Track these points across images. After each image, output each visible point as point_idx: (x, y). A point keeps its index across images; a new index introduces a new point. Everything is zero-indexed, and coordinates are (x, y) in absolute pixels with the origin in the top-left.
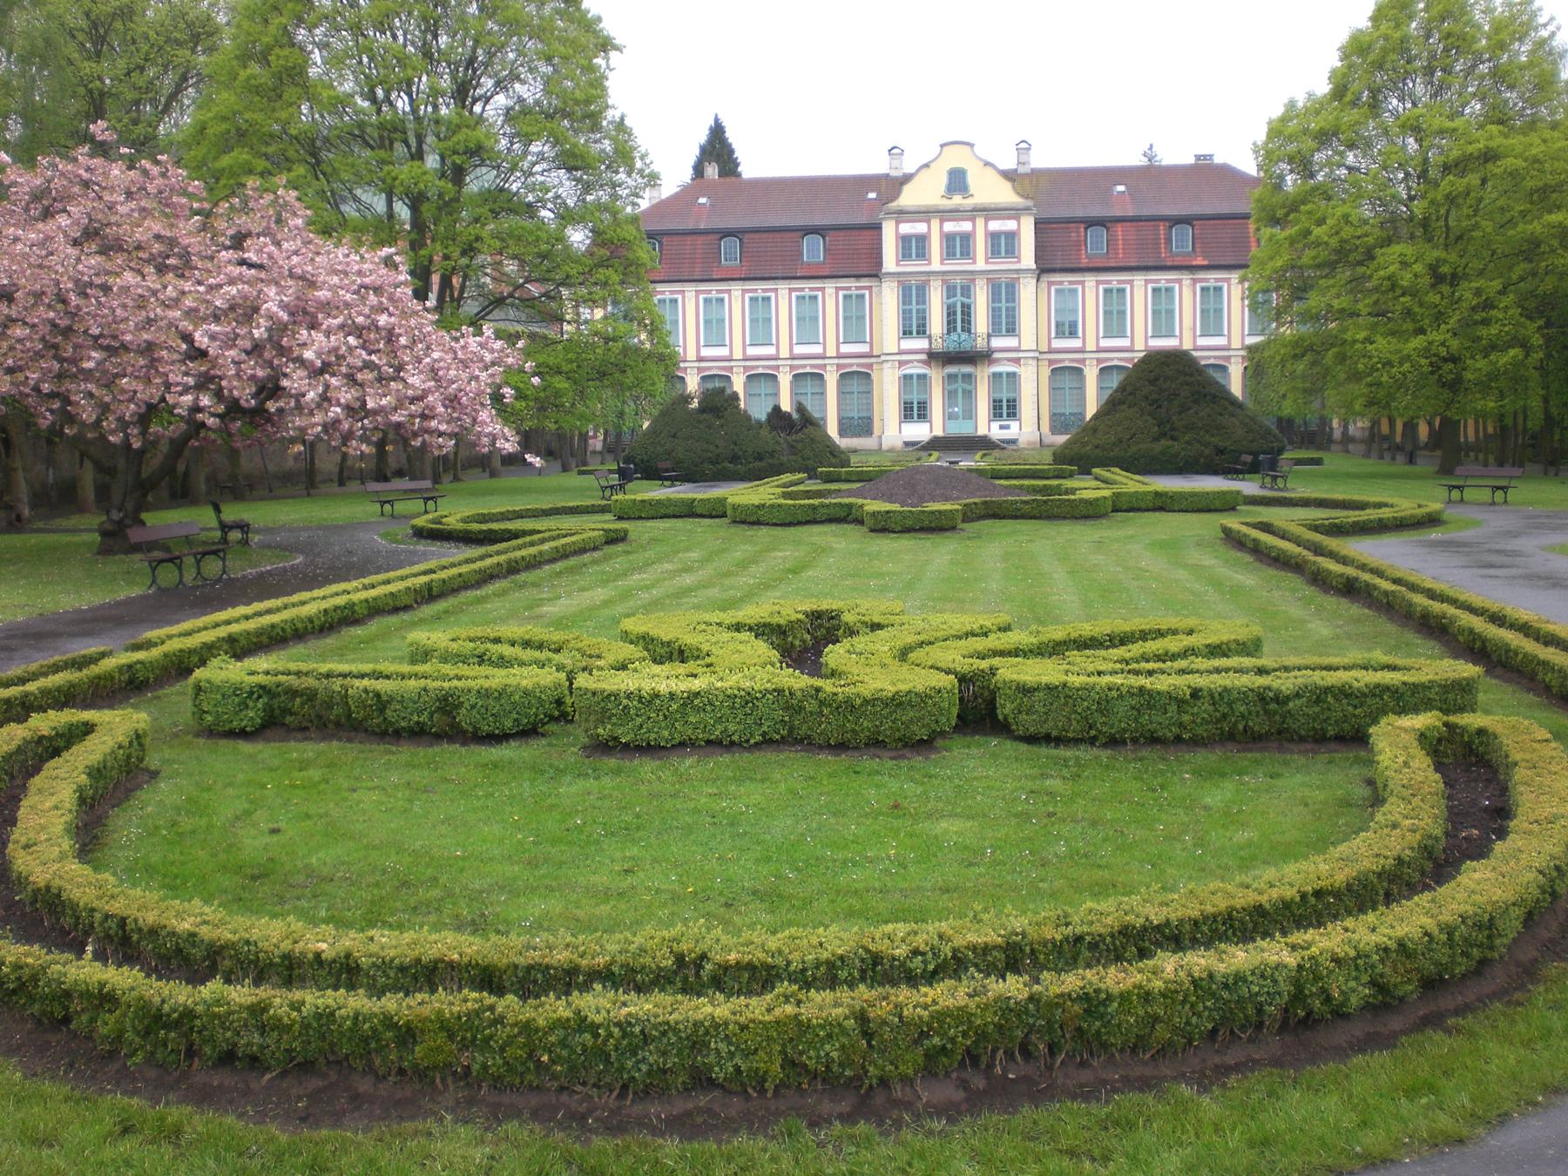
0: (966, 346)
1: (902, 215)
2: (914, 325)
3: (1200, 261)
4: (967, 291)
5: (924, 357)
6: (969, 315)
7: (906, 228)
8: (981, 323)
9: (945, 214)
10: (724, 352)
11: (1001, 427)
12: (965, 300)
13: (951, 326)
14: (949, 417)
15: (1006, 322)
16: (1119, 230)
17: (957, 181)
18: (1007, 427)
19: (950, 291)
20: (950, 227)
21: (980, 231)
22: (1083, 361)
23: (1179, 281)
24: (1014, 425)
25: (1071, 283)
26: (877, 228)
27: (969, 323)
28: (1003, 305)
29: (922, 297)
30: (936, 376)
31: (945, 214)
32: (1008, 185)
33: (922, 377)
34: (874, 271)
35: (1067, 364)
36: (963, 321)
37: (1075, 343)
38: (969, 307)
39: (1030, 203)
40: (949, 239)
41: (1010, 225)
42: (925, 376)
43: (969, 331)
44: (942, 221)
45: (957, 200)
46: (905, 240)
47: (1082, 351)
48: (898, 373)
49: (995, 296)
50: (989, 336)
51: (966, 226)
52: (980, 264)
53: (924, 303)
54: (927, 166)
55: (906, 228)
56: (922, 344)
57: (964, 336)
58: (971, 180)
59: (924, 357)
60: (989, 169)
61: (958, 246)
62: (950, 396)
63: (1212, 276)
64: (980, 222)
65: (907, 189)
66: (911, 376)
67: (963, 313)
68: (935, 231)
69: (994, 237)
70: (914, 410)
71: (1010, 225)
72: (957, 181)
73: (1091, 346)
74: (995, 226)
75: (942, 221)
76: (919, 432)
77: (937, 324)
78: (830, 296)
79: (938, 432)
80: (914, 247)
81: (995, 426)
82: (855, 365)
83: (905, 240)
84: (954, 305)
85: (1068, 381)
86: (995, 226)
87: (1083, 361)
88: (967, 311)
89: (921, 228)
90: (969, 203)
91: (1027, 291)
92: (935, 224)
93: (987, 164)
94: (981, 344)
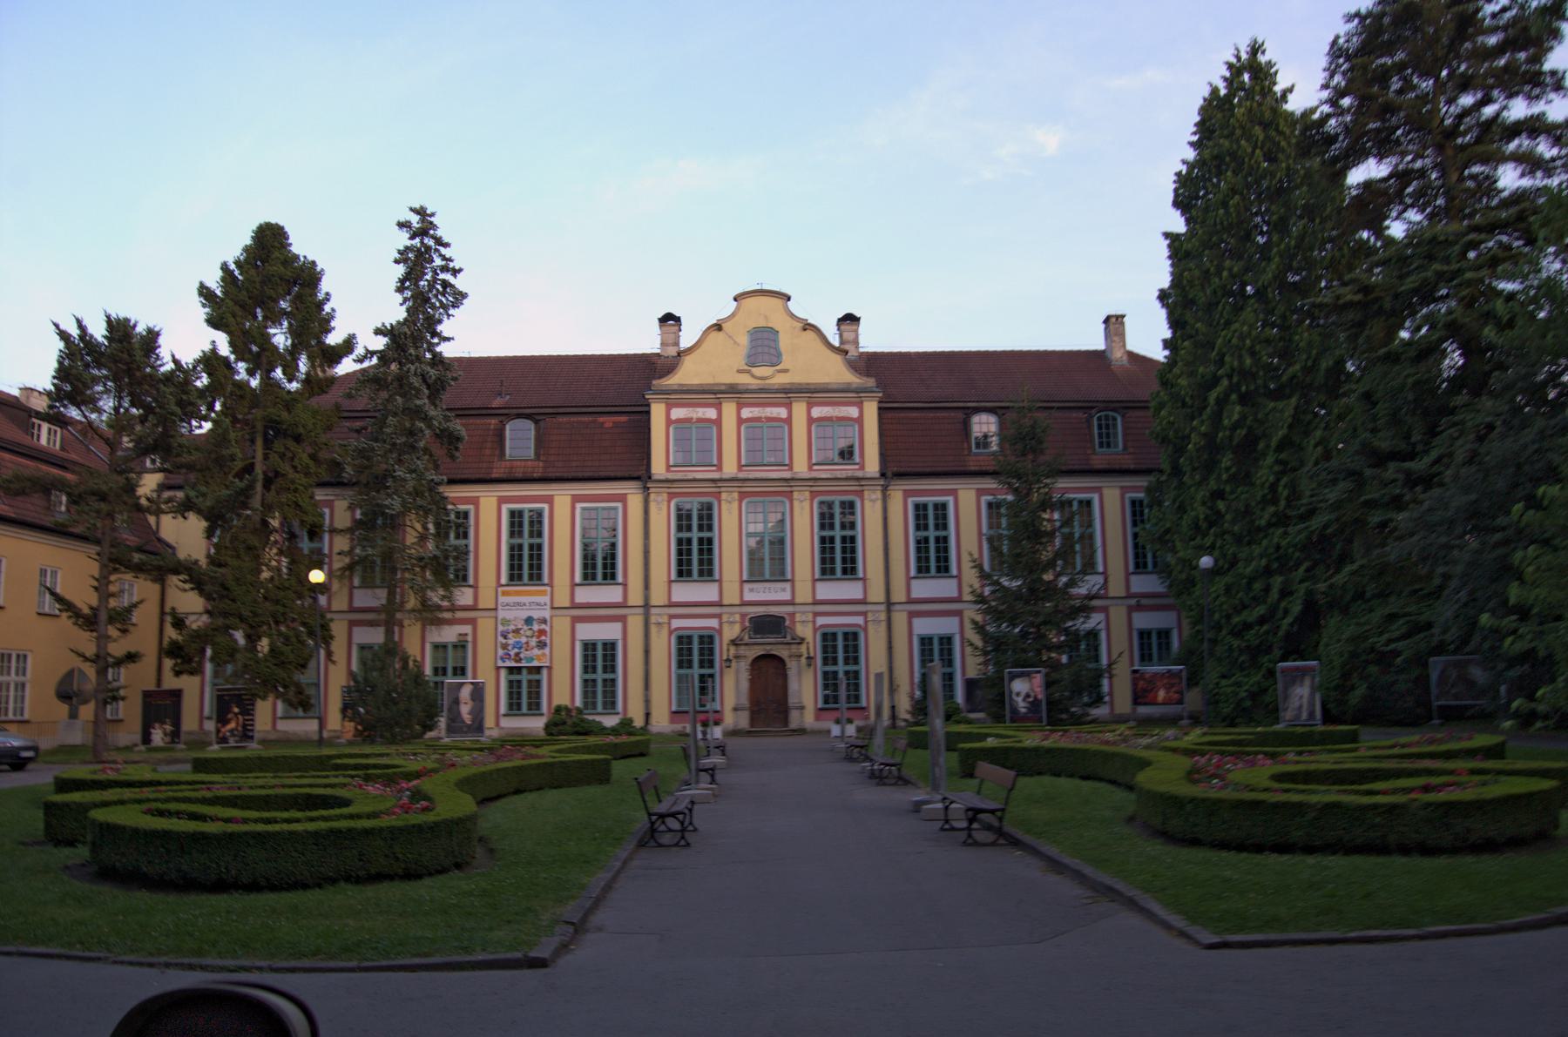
17: (764, 345)
26: (648, 413)
32: (838, 358)
34: (640, 474)
39: (871, 382)
44: (740, 406)
58: (784, 342)
60: (810, 334)
64: (799, 409)
72: (764, 345)
75: (740, 406)
78: (565, 512)
90: (780, 380)
91: (870, 512)
92: (729, 409)
93: (808, 327)
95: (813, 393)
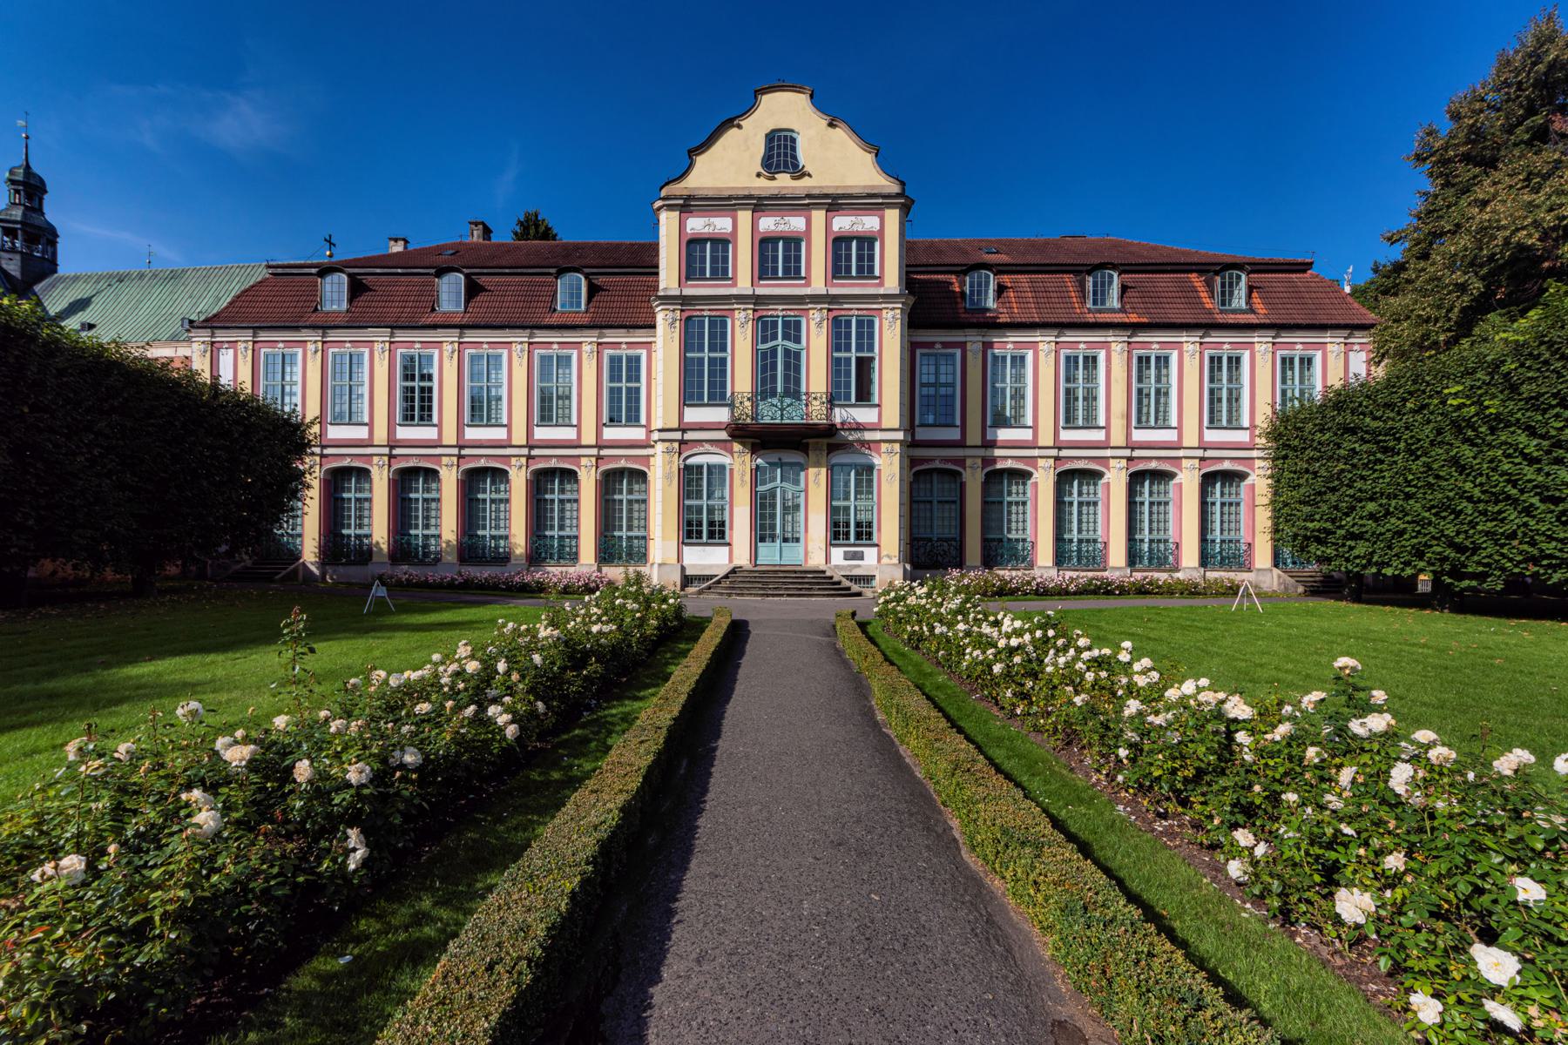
0: (795, 416)
1: (688, 205)
2: (702, 380)
3: (1134, 318)
4: (793, 330)
5: (723, 435)
6: (797, 369)
7: (697, 225)
8: (816, 378)
9: (760, 204)
10: (428, 433)
11: (847, 556)
12: (791, 345)
13: (764, 387)
14: (763, 531)
15: (857, 381)
16: (1006, 279)
17: (780, 152)
18: (861, 557)
19: (765, 329)
20: (768, 224)
21: (818, 229)
22: (961, 462)
23: (1106, 345)
24: (870, 554)
25: (945, 345)
27: (798, 382)
28: (853, 355)
29: (719, 341)
30: (739, 463)
31: (760, 204)
32: (868, 158)
33: (717, 471)
35: (937, 465)
36: (787, 378)
37: (954, 434)
38: (797, 355)
40: (765, 244)
41: (869, 223)
42: (722, 467)
43: (796, 395)
45: (784, 181)
46: (693, 245)
47: (961, 444)
48: (676, 462)
49: (838, 339)
50: (832, 401)
51: (796, 223)
52: (818, 285)
53: (724, 349)
54: (729, 123)
55: (697, 225)
56: (721, 415)
57: (788, 401)
59: (723, 435)
61: (778, 255)
62: (762, 508)
63: (1156, 338)
65: (701, 161)
66: (700, 467)
67: (787, 366)
68: (742, 228)
69: (839, 242)
70: (700, 527)
71: (869, 223)
72: (780, 152)
73: (974, 437)
74: (843, 223)
76: (708, 559)
77: (741, 379)
79: (742, 559)
80: (705, 256)
81: (838, 554)
82: (622, 460)
83: (693, 245)
84: (774, 350)
85: (939, 488)
86: (843, 223)
87: (961, 462)
88: (793, 361)
89: (722, 224)
94: (817, 413)
95: (835, 203)
